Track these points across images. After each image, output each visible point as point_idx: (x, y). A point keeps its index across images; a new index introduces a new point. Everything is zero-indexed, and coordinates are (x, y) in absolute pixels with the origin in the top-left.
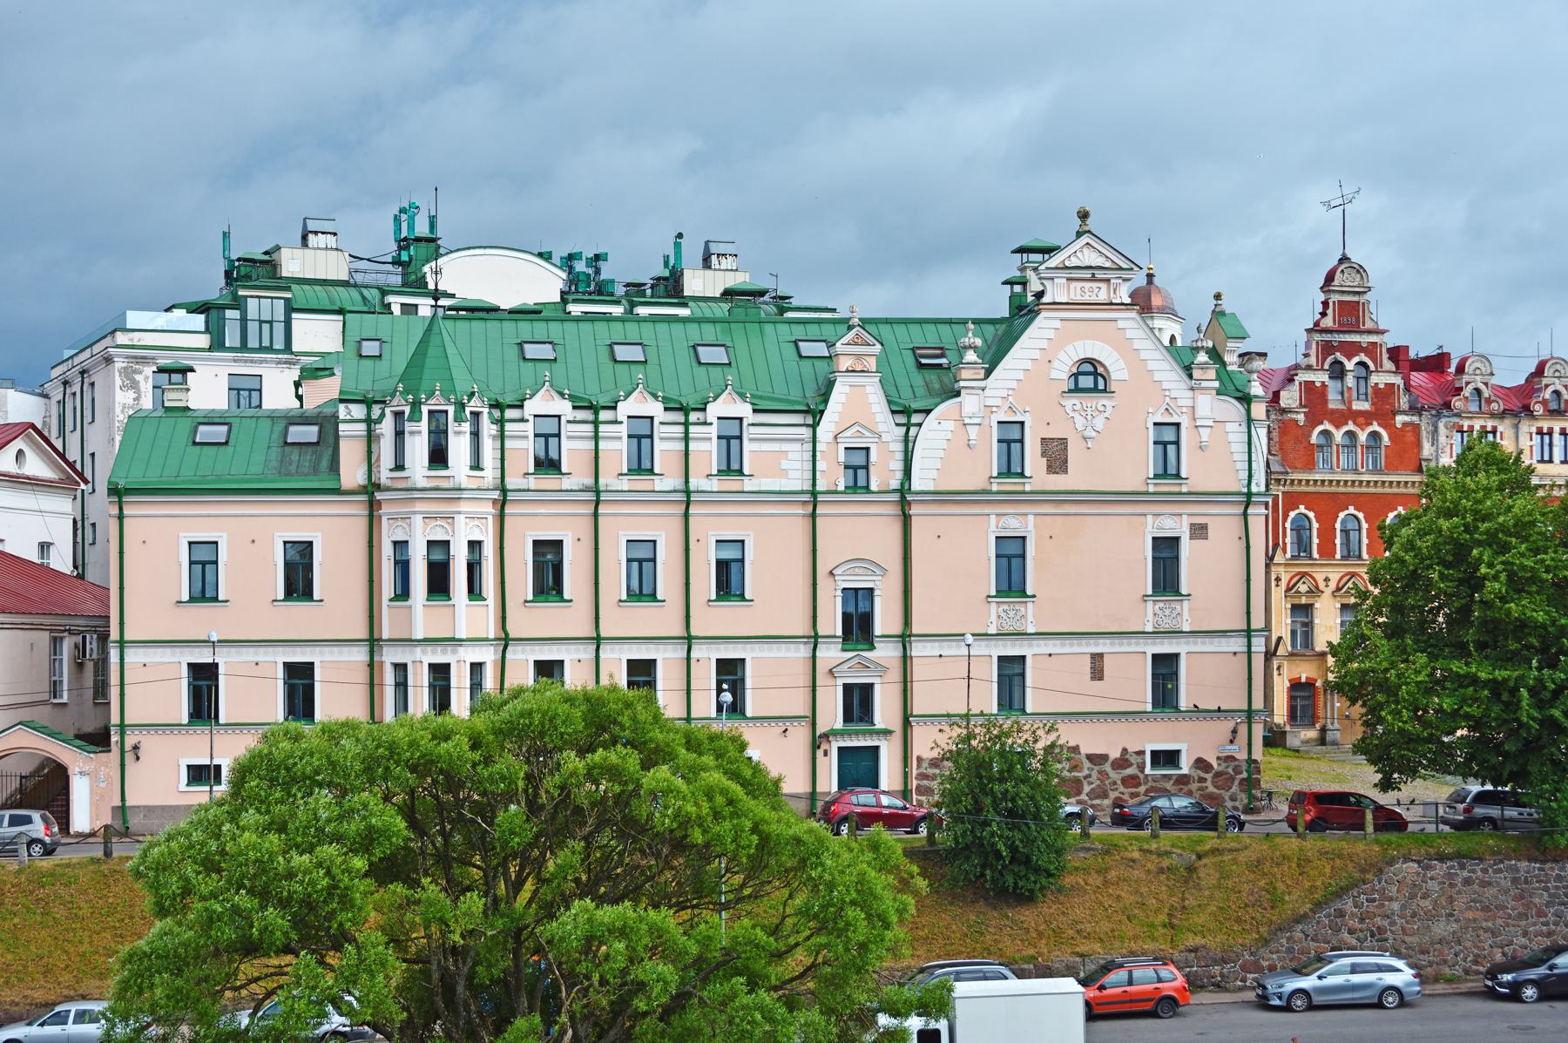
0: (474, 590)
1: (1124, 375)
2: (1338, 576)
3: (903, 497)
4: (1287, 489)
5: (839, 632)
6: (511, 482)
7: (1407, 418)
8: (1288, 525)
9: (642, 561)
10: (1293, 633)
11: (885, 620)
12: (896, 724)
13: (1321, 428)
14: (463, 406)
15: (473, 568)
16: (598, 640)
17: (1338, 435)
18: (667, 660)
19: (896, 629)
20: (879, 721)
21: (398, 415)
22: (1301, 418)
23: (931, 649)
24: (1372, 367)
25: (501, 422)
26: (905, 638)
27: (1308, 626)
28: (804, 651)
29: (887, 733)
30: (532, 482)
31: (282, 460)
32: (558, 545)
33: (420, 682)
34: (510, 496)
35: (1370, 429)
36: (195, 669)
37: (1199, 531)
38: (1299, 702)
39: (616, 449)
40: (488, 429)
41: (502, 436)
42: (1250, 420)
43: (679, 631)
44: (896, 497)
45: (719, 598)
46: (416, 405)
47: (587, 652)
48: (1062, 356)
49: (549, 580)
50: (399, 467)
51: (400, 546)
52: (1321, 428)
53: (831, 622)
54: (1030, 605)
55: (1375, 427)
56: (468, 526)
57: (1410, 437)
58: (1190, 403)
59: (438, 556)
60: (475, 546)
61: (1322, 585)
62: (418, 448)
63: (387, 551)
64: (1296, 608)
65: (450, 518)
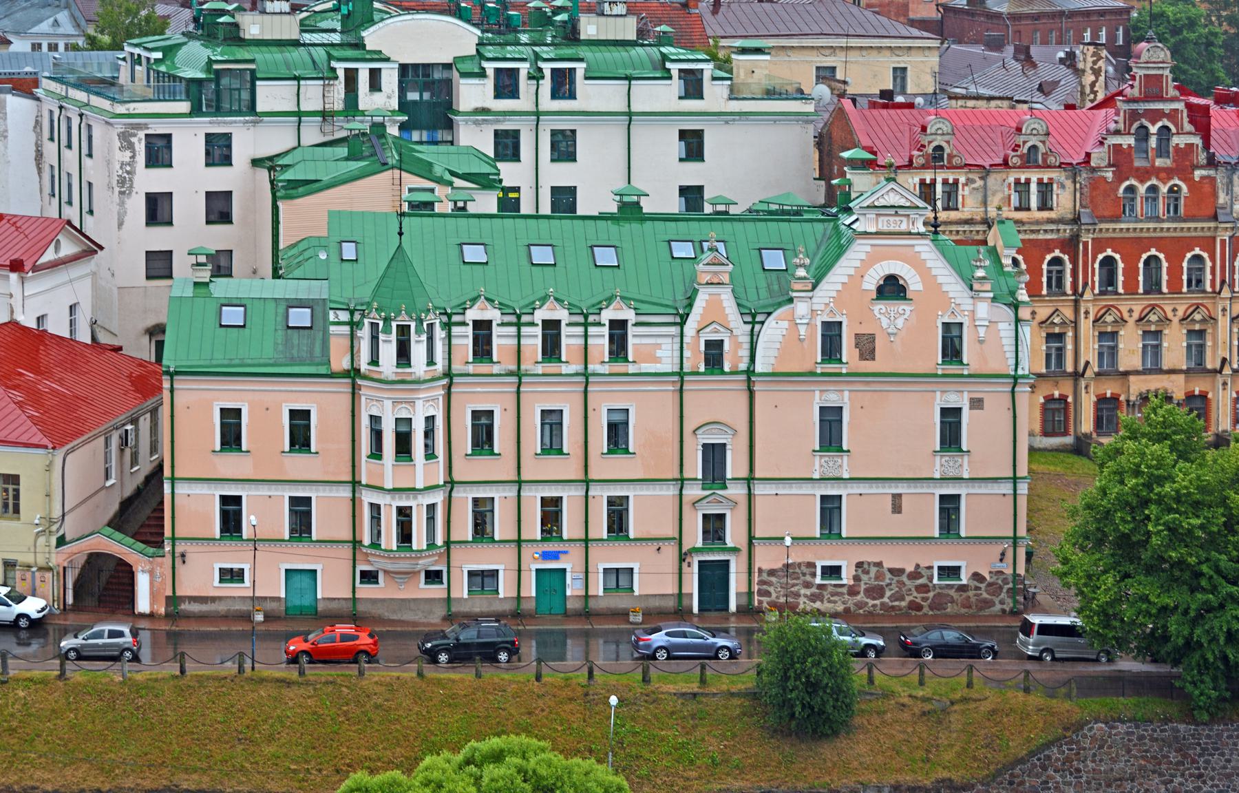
0: (430, 454)
1: (919, 287)
3: (749, 378)
4: (1095, 236)
5: (700, 476)
6: (457, 367)
8: (1097, 266)
9: (552, 421)
10: (1101, 355)
11: (734, 466)
12: (742, 543)
13: (1127, 183)
14: (421, 321)
15: (429, 433)
16: (520, 483)
17: (1142, 189)
18: (570, 497)
19: (744, 473)
20: (730, 542)
21: (374, 326)
22: (1109, 175)
23: (769, 489)
25: (447, 326)
26: (750, 480)
27: (1113, 351)
28: (672, 491)
29: (735, 550)
30: (471, 369)
31: (287, 341)
32: (490, 413)
33: (390, 523)
34: (456, 380)
35: (1172, 183)
36: (225, 500)
37: (977, 404)
38: (1105, 413)
39: (534, 339)
40: (439, 334)
41: (449, 336)
42: (1018, 320)
43: (581, 476)
44: (743, 377)
45: (610, 452)
46: (387, 320)
47: (511, 492)
48: (871, 271)
49: (483, 437)
50: (374, 361)
51: (375, 420)
52: (1127, 183)
53: (695, 467)
54: (845, 458)
56: (424, 407)
57: (1207, 188)
58: (971, 308)
59: (403, 429)
60: (430, 420)
61: (1126, 316)
62: (388, 351)
63: (365, 422)
64: (1102, 335)
65: (412, 403)
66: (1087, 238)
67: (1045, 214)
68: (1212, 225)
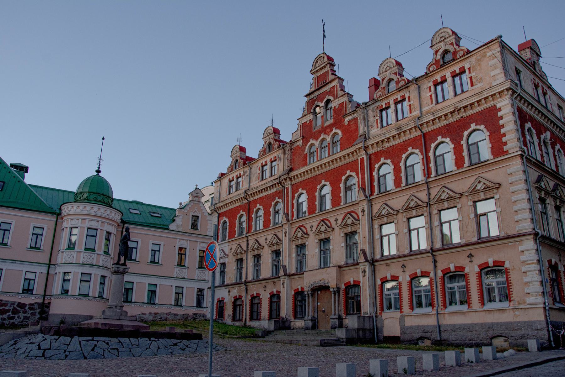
2: (317, 223)
7: (350, 118)
13: (310, 143)
22: (300, 143)
24: (331, 98)
52: (310, 143)
55: (334, 130)
66: (288, 185)
67: (273, 178)
68: (352, 149)
